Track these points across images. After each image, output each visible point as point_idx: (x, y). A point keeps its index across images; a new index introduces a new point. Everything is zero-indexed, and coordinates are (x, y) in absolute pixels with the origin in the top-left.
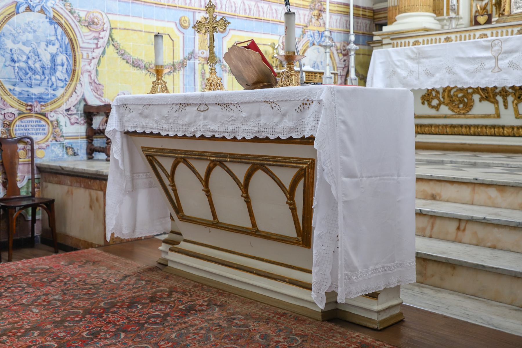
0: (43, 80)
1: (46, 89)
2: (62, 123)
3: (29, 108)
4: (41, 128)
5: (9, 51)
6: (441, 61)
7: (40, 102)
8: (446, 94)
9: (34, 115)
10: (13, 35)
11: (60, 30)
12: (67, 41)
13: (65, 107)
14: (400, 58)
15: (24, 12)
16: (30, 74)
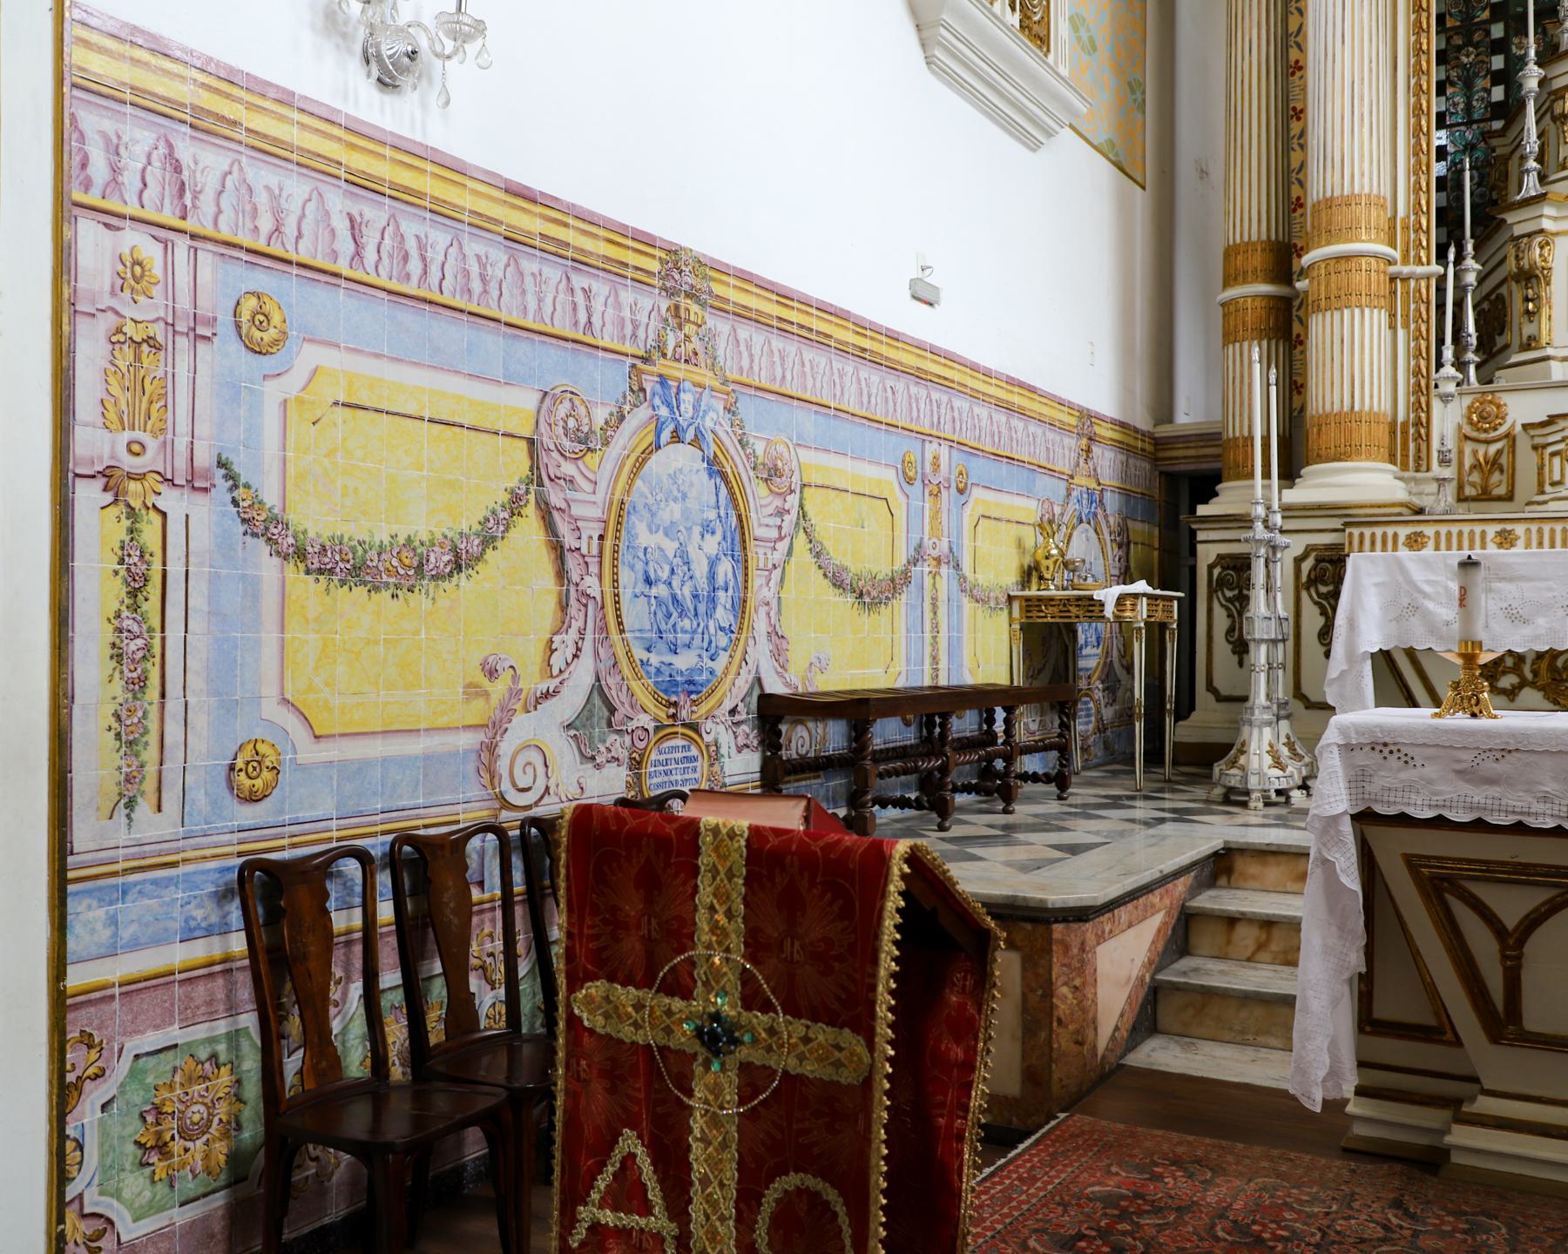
0: (694, 632)
1: (700, 656)
2: (724, 751)
3: (672, 711)
4: (691, 765)
5: (641, 554)
6: (1550, 589)
7: (690, 693)
8: (1544, 665)
9: (680, 730)
10: (650, 510)
11: (723, 491)
12: (734, 521)
13: (728, 705)
14: (1433, 578)
15: (668, 444)
16: (675, 615)
